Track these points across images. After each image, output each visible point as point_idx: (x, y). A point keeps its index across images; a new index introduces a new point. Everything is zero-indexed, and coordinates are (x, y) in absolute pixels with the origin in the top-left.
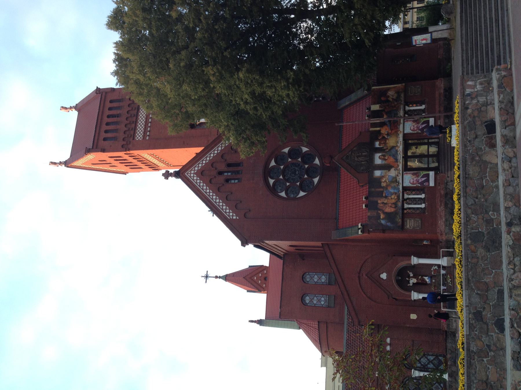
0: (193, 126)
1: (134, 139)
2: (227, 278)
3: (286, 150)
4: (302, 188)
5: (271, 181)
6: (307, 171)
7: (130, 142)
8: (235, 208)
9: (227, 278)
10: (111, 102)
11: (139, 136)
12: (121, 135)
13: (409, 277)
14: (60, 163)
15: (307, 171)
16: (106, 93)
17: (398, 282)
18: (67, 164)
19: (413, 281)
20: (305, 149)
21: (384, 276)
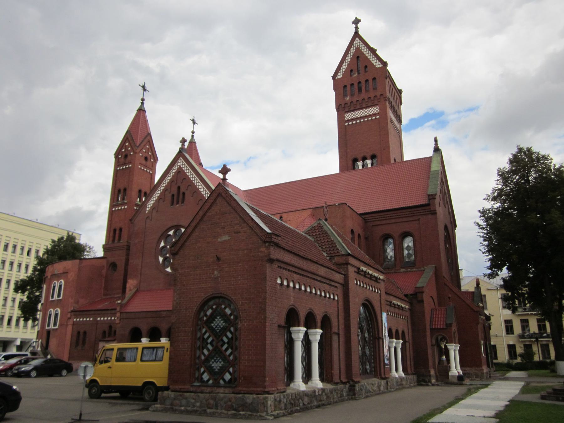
2: (141, 111)
9: (141, 111)
14: (357, 28)
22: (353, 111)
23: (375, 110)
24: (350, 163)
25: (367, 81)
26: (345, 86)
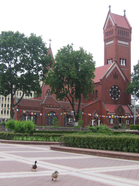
0: (120, 59)
1: (118, 40)
3: (119, 91)
4: (112, 95)
5: (113, 87)
6: (115, 97)
8: (108, 77)
10: (128, 32)
11: (119, 42)
14: (110, 9)
15: (115, 97)
18: (110, 11)
20: (119, 96)
22: (108, 42)
23: (112, 42)
24: (107, 61)
25: (111, 31)
26: (106, 33)
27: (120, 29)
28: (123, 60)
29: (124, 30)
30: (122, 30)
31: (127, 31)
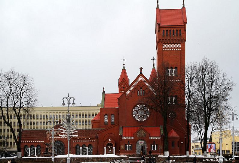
0: (168, 68)
1: (163, 44)
7: (162, 42)
8: (129, 95)
11: (164, 46)
12: (165, 38)
13: (111, 146)
14: (158, 5)
16: (184, 27)
17: (109, 143)
18: (158, 8)
19: (110, 147)
21: (110, 140)
27: (165, 29)
28: (172, 68)
29: (172, 29)
30: (169, 29)
31: (179, 29)
